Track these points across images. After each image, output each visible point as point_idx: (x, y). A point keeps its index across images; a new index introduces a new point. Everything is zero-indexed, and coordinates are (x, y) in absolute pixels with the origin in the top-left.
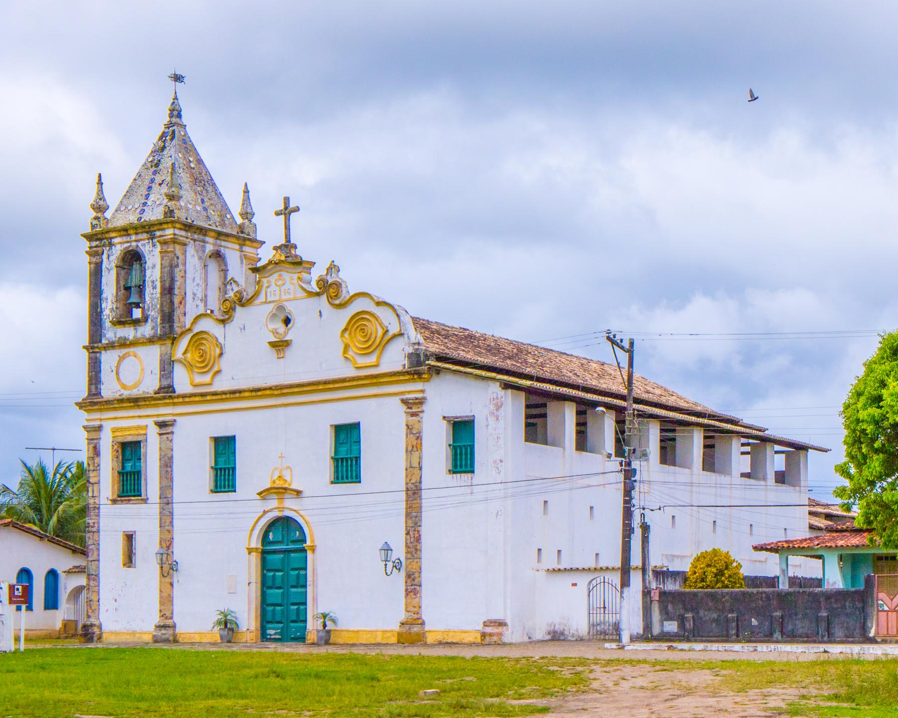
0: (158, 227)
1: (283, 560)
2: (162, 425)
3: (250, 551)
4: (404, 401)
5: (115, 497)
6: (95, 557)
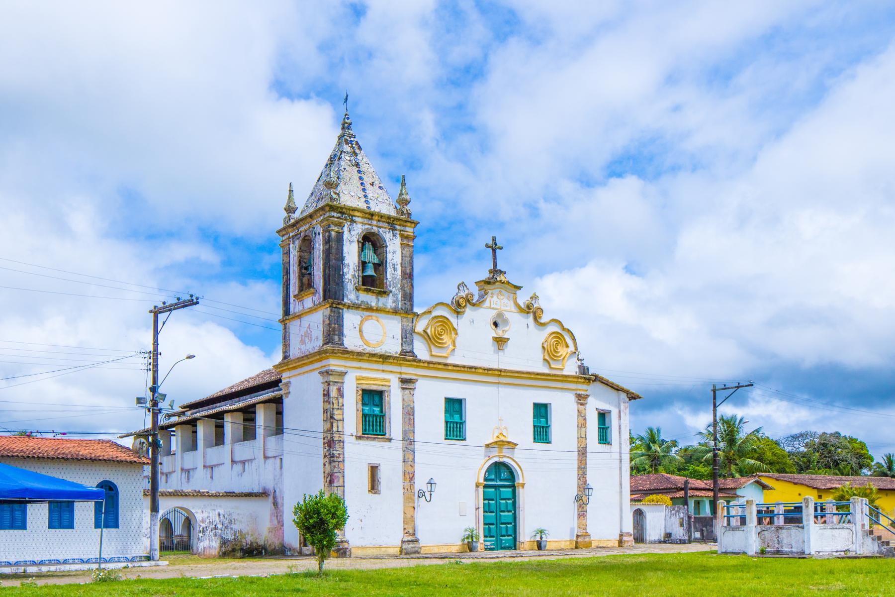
2: (404, 381)
4: (579, 397)
5: (360, 434)
6: (341, 483)
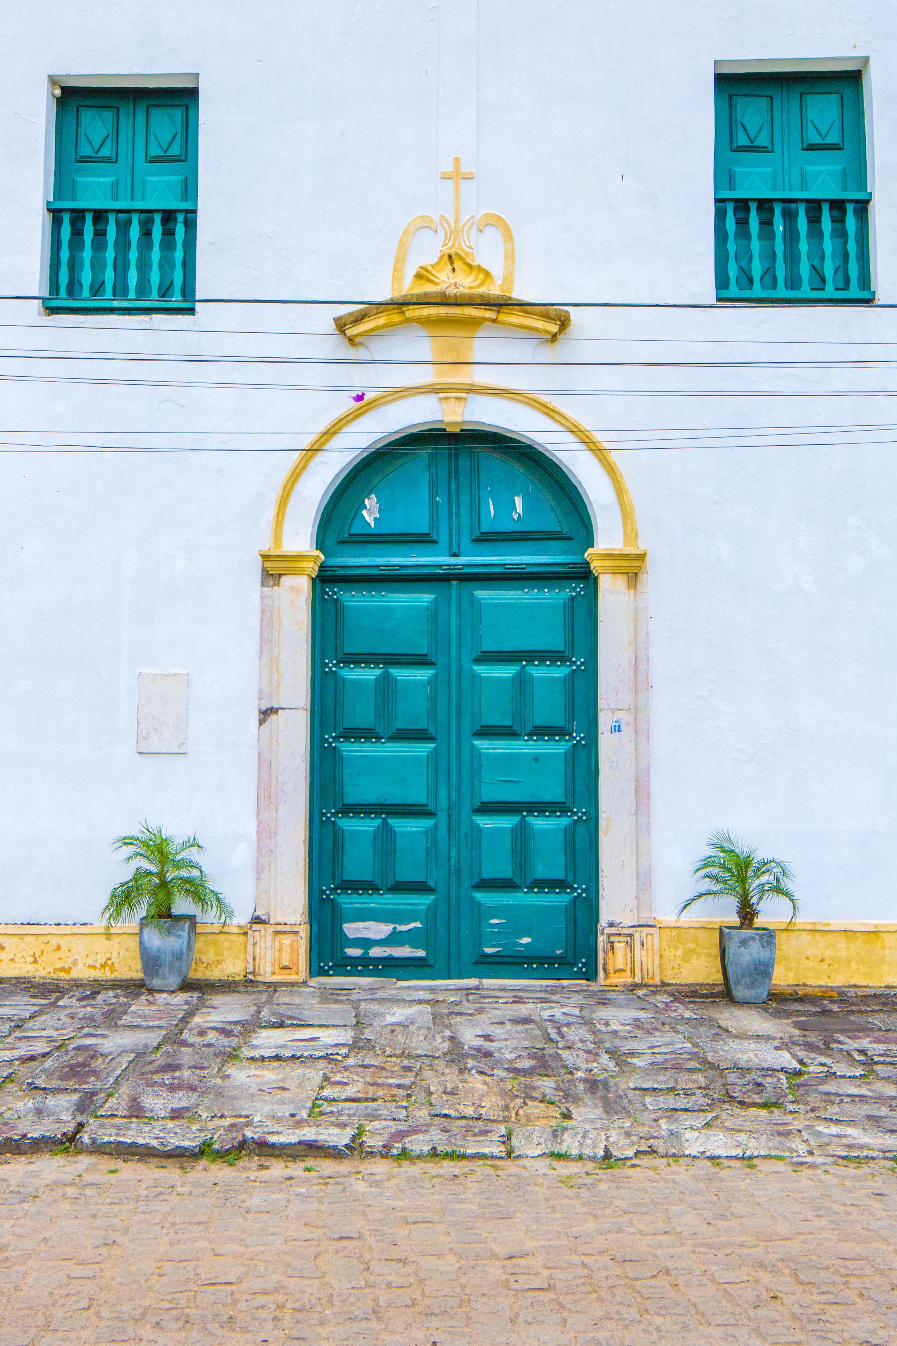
1: (433, 613)
3: (273, 570)
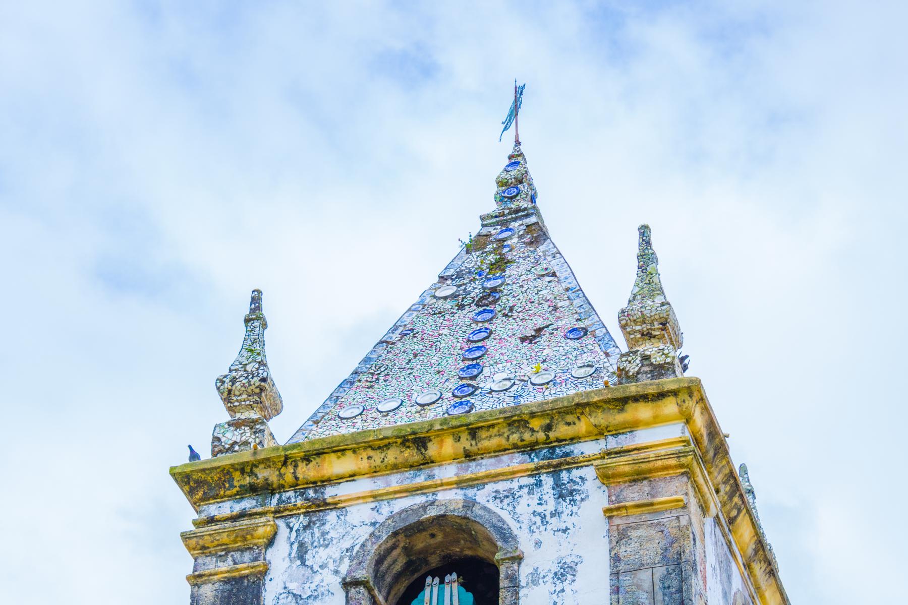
0: (600, 418)
